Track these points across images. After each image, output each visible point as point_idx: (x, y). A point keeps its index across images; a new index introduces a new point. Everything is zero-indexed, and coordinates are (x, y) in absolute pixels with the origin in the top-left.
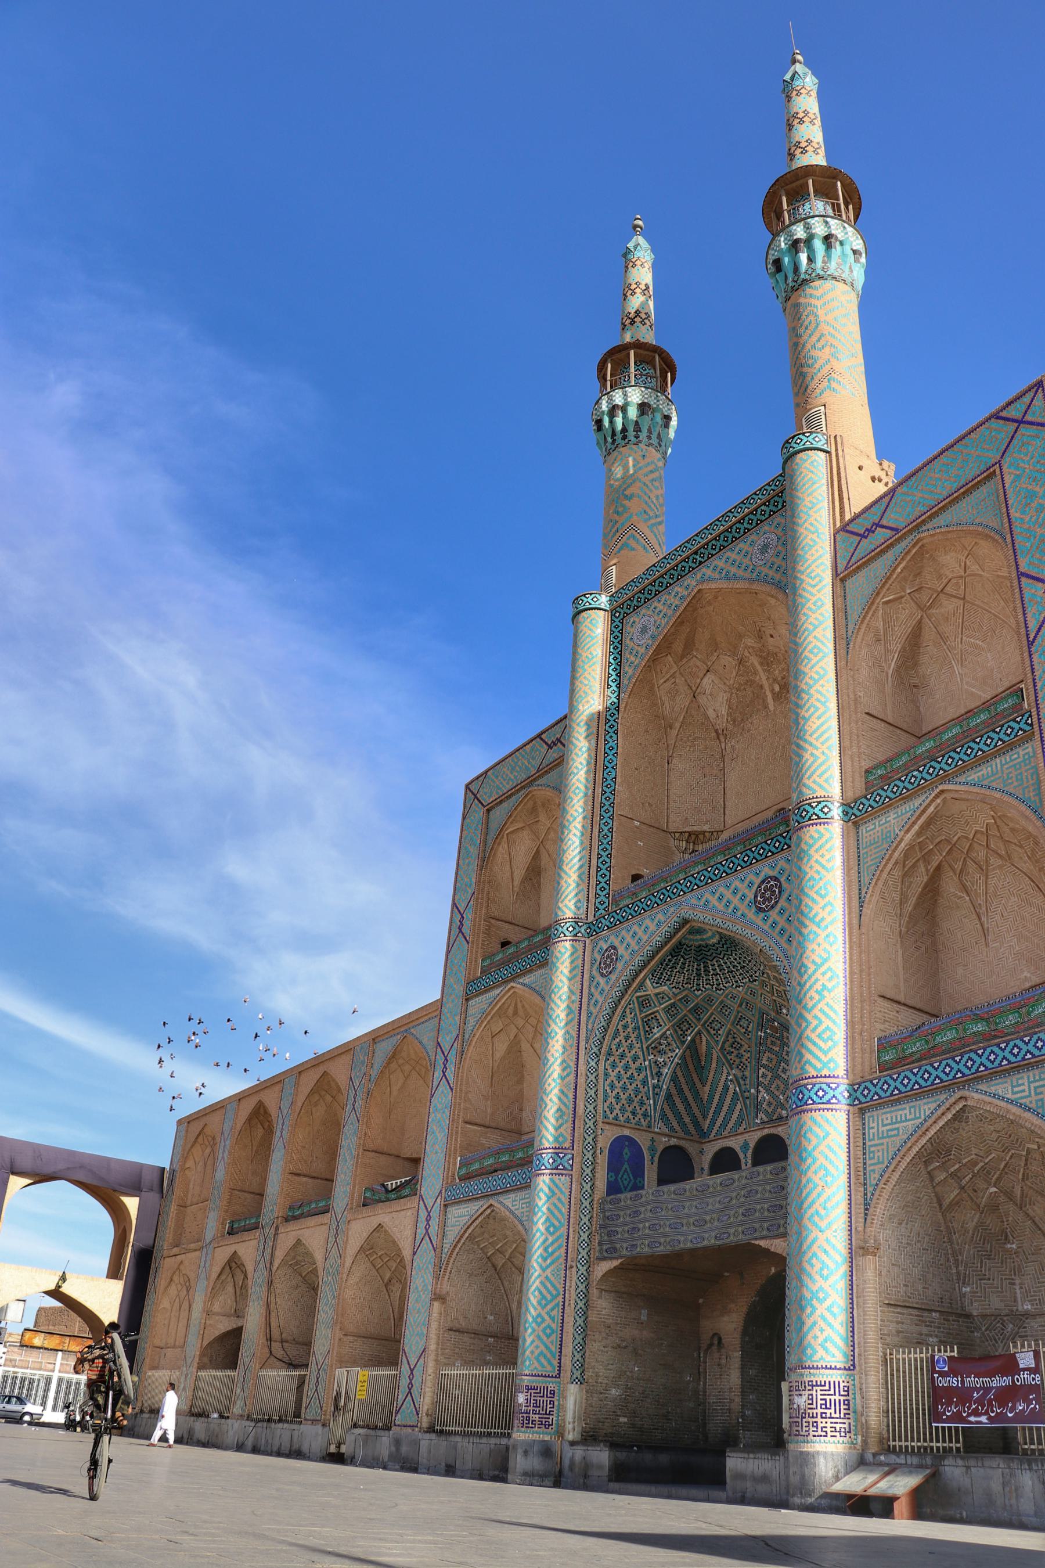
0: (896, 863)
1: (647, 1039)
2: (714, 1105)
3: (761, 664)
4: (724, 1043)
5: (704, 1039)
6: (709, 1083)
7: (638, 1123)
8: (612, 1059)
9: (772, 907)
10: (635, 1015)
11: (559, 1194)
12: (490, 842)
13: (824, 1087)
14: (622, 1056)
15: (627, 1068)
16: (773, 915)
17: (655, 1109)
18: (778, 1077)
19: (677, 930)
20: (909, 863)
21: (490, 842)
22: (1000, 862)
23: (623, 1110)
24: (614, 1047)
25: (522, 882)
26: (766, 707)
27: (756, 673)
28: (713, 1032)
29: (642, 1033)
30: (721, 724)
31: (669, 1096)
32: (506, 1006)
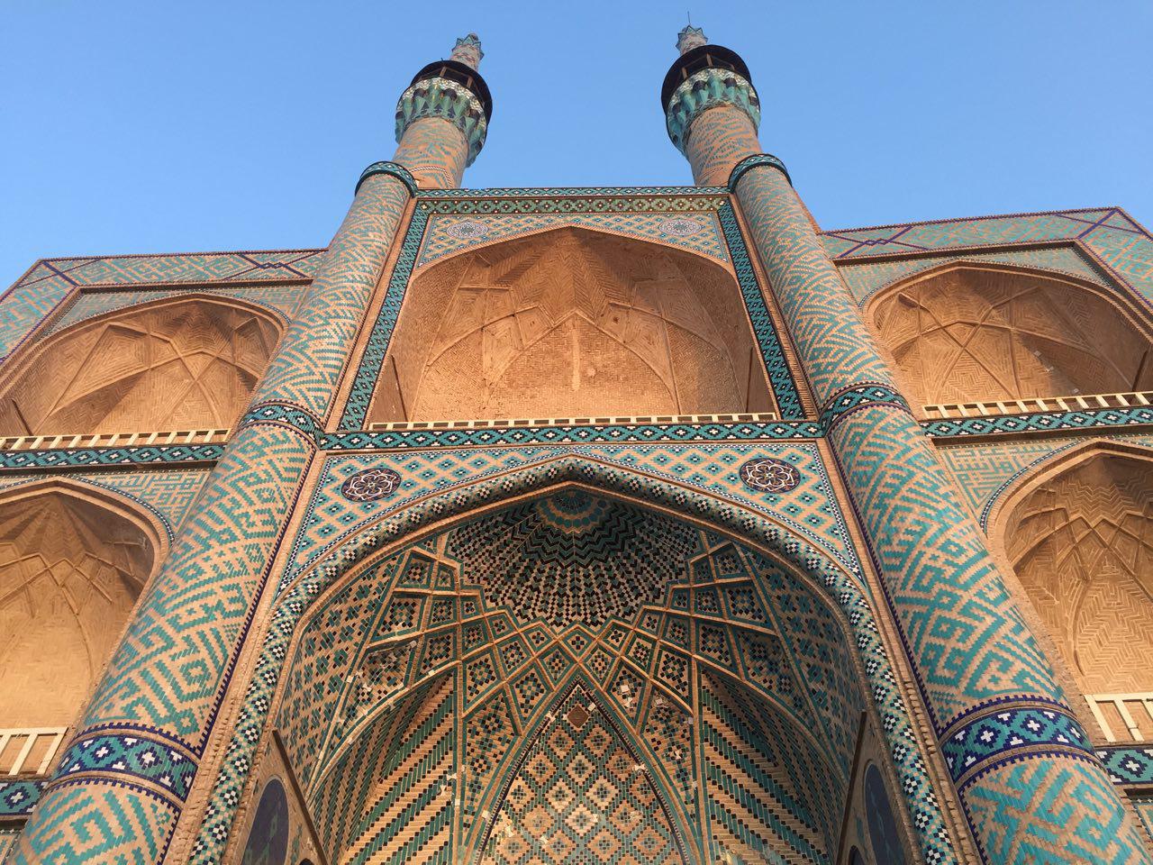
2: (382, 823)
3: (582, 342)
5: (449, 686)
6: (394, 778)
8: (313, 634)
9: (783, 490)
10: (390, 582)
11: (141, 842)
14: (328, 641)
16: (790, 498)
17: (320, 772)
18: (546, 803)
21: (61, 326)
22: (1118, 571)
24: (328, 615)
25: (81, 401)
26: (567, 385)
27: (569, 347)
28: (470, 683)
29: (376, 622)
30: (493, 377)
32: (14, 510)
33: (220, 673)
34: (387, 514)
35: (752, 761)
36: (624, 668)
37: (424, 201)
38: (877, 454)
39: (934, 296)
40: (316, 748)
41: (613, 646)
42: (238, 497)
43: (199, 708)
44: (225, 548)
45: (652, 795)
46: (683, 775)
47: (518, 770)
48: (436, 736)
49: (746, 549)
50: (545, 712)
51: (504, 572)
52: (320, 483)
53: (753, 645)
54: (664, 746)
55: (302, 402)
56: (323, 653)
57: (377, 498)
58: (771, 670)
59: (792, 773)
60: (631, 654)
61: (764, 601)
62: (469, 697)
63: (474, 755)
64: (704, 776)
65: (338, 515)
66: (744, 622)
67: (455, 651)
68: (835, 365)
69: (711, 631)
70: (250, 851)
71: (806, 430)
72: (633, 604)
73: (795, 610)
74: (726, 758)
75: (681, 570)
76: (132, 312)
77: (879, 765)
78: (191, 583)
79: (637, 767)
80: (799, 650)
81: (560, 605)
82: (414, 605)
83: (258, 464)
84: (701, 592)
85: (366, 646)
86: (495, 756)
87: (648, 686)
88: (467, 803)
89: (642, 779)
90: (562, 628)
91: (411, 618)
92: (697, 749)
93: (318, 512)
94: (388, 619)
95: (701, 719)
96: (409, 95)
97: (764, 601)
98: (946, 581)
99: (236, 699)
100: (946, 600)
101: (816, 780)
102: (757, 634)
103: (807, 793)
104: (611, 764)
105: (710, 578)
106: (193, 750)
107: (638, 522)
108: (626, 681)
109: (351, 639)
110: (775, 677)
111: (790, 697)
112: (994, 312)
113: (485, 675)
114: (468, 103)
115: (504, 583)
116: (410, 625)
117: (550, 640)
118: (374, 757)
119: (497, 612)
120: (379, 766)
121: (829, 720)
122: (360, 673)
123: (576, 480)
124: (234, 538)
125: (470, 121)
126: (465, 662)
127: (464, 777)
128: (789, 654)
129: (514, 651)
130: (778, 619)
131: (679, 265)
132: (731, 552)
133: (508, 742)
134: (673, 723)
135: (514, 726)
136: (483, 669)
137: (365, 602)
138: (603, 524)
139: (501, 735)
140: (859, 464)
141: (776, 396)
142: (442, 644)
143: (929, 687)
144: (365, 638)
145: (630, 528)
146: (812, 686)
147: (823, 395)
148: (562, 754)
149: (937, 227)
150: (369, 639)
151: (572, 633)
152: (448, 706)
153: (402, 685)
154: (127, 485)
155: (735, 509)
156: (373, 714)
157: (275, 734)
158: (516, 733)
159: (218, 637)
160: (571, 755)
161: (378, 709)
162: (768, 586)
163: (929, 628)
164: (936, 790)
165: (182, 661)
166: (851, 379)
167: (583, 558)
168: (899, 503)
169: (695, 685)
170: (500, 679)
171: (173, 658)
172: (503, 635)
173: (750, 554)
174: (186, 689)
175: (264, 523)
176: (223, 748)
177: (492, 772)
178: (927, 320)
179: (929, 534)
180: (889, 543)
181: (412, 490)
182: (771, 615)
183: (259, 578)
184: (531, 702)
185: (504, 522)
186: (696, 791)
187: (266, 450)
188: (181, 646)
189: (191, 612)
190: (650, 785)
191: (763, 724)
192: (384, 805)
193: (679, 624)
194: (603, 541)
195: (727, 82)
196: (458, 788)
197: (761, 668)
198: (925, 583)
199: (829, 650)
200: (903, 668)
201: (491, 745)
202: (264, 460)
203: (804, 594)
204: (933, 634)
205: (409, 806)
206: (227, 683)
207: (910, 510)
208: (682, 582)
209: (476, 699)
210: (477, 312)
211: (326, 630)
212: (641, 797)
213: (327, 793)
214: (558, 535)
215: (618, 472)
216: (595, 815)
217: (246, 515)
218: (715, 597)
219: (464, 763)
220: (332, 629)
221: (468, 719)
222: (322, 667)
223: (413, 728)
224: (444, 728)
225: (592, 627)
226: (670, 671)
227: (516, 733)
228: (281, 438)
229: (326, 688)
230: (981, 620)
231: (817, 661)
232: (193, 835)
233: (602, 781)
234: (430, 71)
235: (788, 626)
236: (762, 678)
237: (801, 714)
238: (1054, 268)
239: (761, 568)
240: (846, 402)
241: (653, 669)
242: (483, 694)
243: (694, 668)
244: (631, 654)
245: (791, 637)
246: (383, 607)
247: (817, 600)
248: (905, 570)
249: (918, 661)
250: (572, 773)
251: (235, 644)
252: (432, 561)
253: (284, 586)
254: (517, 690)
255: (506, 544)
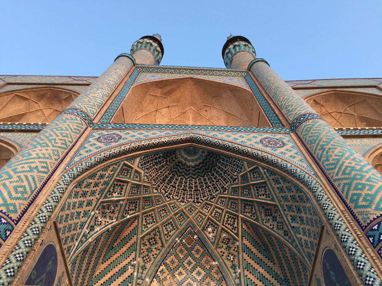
3: (193, 118)
4: (146, 235)
5: (136, 224)
8: (78, 189)
9: (278, 147)
10: (114, 174)
14: (84, 194)
16: (283, 149)
17: (75, 252)
24: (85, 183)
28: (144, 223)
29: (106, 190)
33: (32, 192)
34: (114, 148)
35: (264, 262)
36: (209, 221)
37: (138, 67)
38: (318, 133)
39: (326, 102)
40: (74, 240)
41: (205, 211)
42: (52, 133)
43: (20, 204)
44: (43, 149)
45: (220, 275)
46: (234, 267)
47: (163, 262)
48: (128, 245)
49: (264, 168)
50: (176, 238)
51: (162, 178)
52: (88, 137)
53: (266, 210)
54: (226, 254)
55: (84, 110)
56: (82, 199)
57: (111, 142)
58: (273, 220)
59: (281, 267)
60: (213, 215)
61: (271, 190)
62: (143, 229)
63: (144, 254)
64: (243, 267)
65: (94, 146)
66: (262, 199)
67: (139, 209)
68: (296, 109)
69: (247, 204)
70: (35, 272)
71: (286, 130)
72: (214, 194)
73: (285, 192)
74: (253, 260)
75: (235, 179)
76: (25, 91)
77: (333, 247)
78: (25, 158)
79: (214, 263)
80: (287, 209)
81: (184, 194)
82: (123, 186)
83: (63, 125)
84: (244, 188)
85: (101, 200)
86: (153, 255)
87: (220, 228)
88: (140, 275)
89: (216, 268)
90: (184, 203)
91: (121, 191)
92: (240, 255)
93: (86, 145)
94: (112, 191)
95: (242, 242)
96: (136, 44)
97: (271, 190)
98: (357, 171)
99: (38, 205)
100: (358, 177)
101: (294, 268)
102: (268, 204)
103: (289, 275)
104: (203, 262)
105: (248, 182)
106: (13, 221)
107: (217, 160)
108: (210, 226)
109: (95, 196)
110: (275, 223)
111: (282, 231)
112: (348, 109)
113: (151, 220)
114: (156, 48)
115: (161, 183)
116: (121, 194)
117: (179, 208)
118: (100, 251)
119: (158, 194)
120: (102, 256)
121: (301, 239)
122: (97, 212)
123: (193, 142)
124: (48, 146)
125: (156, 53)
126: (143, 213)
127: (139, 263)
128: (282, 212)
129: (164, 212)
130: (277, 197)
131: (230, 90)
132: (257, 170)
133: (159, 250)
134: (230, 245)
135: (162, 243)
136: (150, 218)
137: (102, 181)
138: (203, 161)
139: (156, 247)
140: (310, 137)
141: (271, 123)
142: (134, 205)
143: (355, 211)
144: (101, 196)
145: (215, 162)
146: (293, 225)
147: (291, 119)
148: (182, 256)
149: (325, 81)
150: (103, 197)
151: (189, 206)
152: (135, 232)
153: (115, 220)
154: (9, 136)
155: (259, 152)
156: (101, 231)
157: (55, 223)
158: (163, 246)
159: (34, 179)
160: (186, 257)
161: (104, 229)
162: (273, 183)
163: (352, 188)
164: (366, 253)
165: (15, 184)
166: (303, 112)
167: (195, 175)
168: (330, 147)
169: (240, 228)
170: (157, 223)
171: (11, 182)
172: (159, 204)
173: (265, 170)
174: (14, 195)
175: (62, 144)
176: (28, 223)
177: (151, 262)
178: (324, 110)
179: (346, 155)
180: (328, 160)
181: (126, 140)
182: (274, 196)
183: (57, 162)
184: (170, 234)
185: (163, 157)
186: (240, 274)
187: (67, 121)
188: (15, 178)
189: (23, 168)
190: (220, 270)
191: (269, 245)
192: (103, 274)
193: (233, 202)
194: (203, 168)
195: (245, 45)
196: (136, 268)
197: (269, 220)
198: (347, 172)
199: (301, 208)
200: (340, 206)
201: (151, 251)
202: (65, 124)
203: (289, 185)
204: (354, 189)
205: (114, 274)
206: (35, 198)
207: (336, 149)
208: (236, 184)
209: (147, 230)
210: (155, 104)
211: (84, 189)
212: (216, 276)
213: (78, 262)
214: (184, 165)
215: (211, 139)
216: (195, 283)
217: (55, 139)
218: (249, 190)
219: (139, 257)
220: (86, 190)
221: (142, 238)
222: (81, 205)
223: (119, 241)
224: (132, 241)
225: (197, 204)
226: (229, 222)
227: (163, 246)
228: (74, 119)
229: (82, 215)
230: (377, 183)
231: (295, 214)
232: (5, 256)
233: (199, 269)
234: (144, 38)
235: (282, 200)
236: (269, 224)
237: (287, 238)
238: (370, 92)
239: (270, 176)
240: (302, 119)
241: (222, 221)
242: (150, 228)
243: (240, 221)
244: (213, 215)
245: (283, 205)
246: (110, 185)
247: (296, 186)
248: (337, 169)
249: (348, 201)
250: (186, 265)
251: (41, 184)
252: (132, 168)
253: (67, 168)
254: (164, 228)
255: (163, 166)
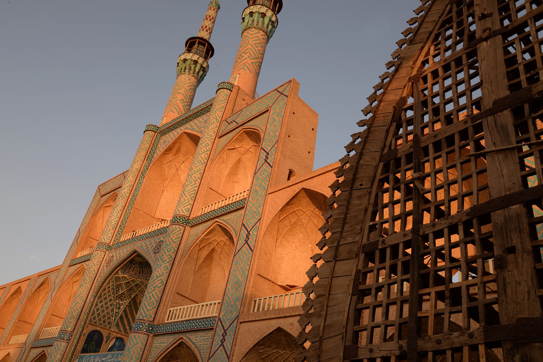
0: (197, 245)
1: (117, 294)
7: (105, 326)
8: (101, 299)
12: (98, 209)
13: (143, 324)
14: (105, 299)
15: (106, 303)
16: (158, 255)
19: (132, 254)
20: (202, 246)
23: (100, 320)
24: (103, 295)
31: (121, 317)
